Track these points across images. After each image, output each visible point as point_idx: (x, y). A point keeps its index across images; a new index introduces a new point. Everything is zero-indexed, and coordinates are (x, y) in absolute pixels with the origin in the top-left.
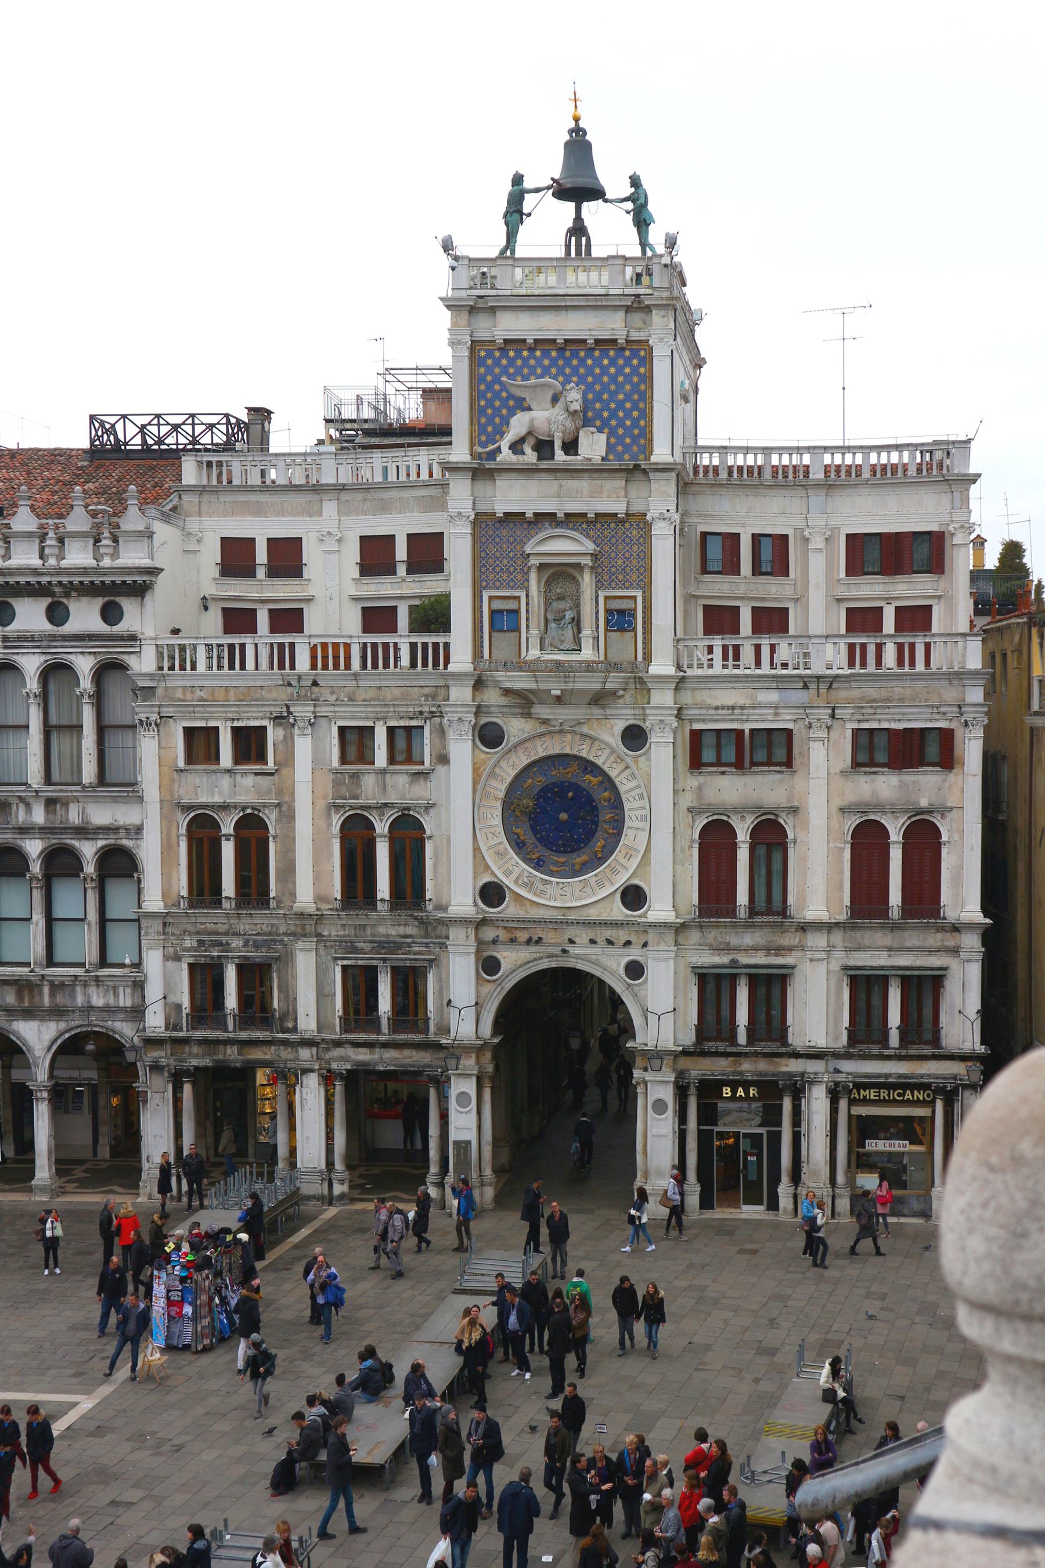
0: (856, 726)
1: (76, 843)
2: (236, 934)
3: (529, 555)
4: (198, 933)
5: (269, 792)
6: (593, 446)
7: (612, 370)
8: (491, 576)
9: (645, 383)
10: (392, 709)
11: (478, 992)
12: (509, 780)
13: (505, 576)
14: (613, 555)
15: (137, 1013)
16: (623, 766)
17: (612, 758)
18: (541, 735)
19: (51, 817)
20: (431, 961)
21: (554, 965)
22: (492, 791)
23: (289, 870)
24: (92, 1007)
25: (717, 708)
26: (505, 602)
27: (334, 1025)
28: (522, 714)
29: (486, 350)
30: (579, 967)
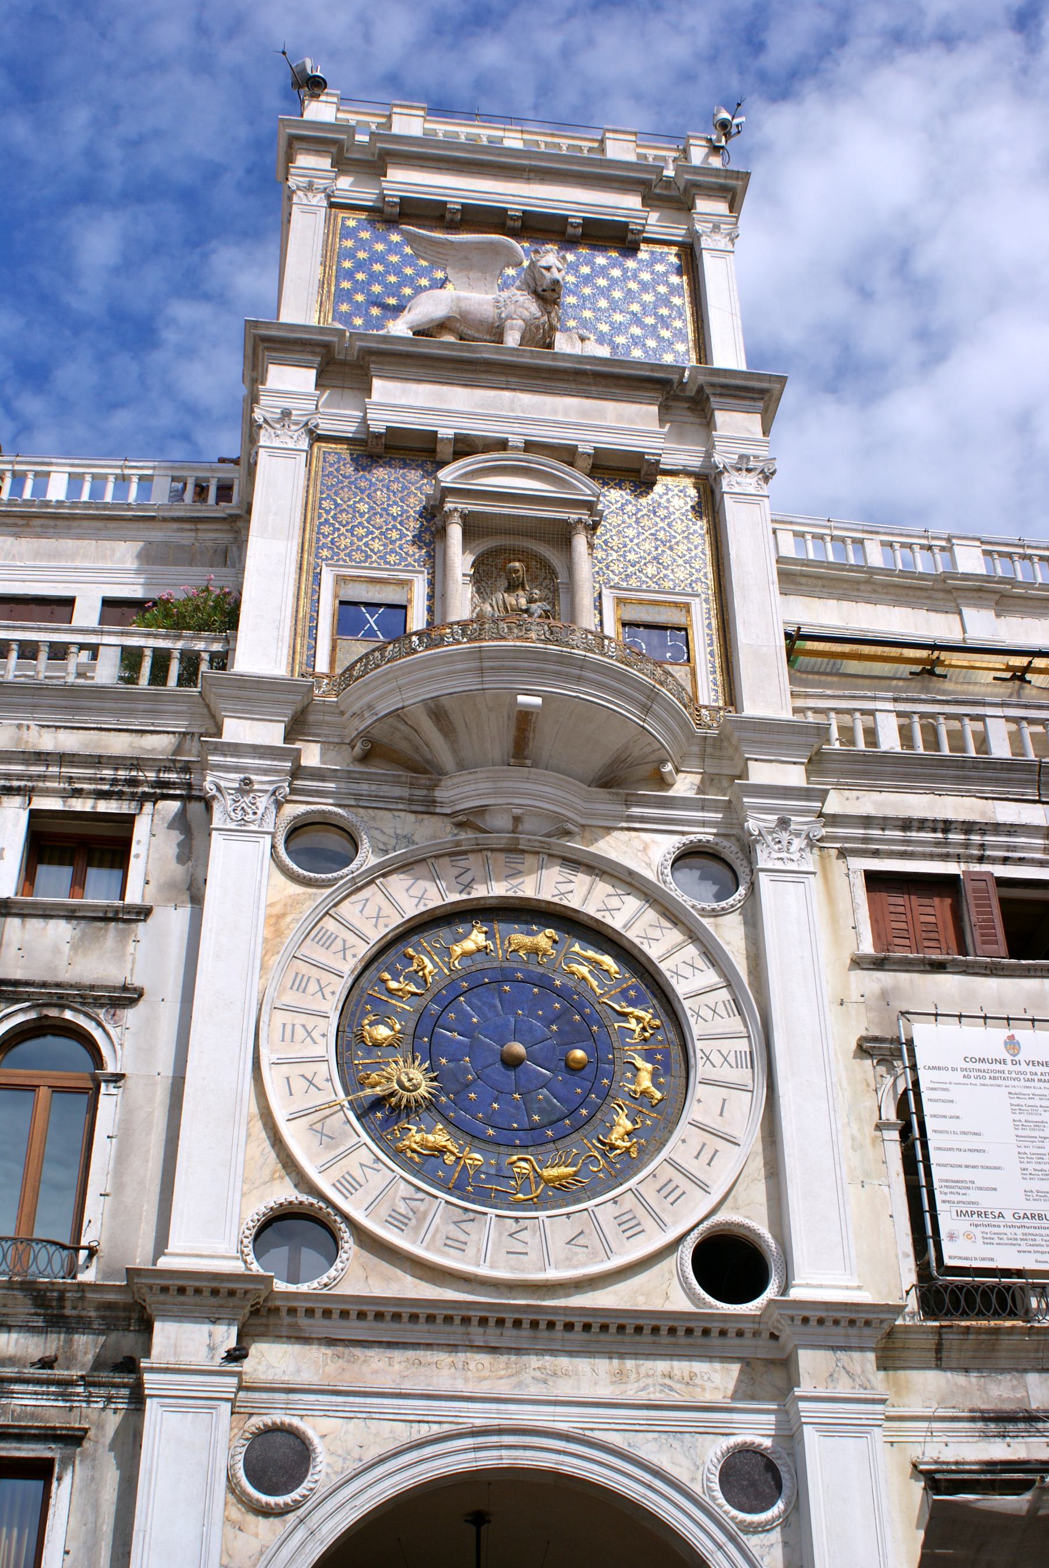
3: (447, 492)
8: (344, 542)
10: (54, 770)
11: (226, 1551)
12: (363, 950)
13: (376, 545)
14: (631, 533)
18: (455, 853)
20: (74, 1439)
21: (488, 1459)
22: (315, 972)
25: (906, 824)
26: (378, 586)
28: (411, 801)
29: (358, 220)
30: (570, 1466)
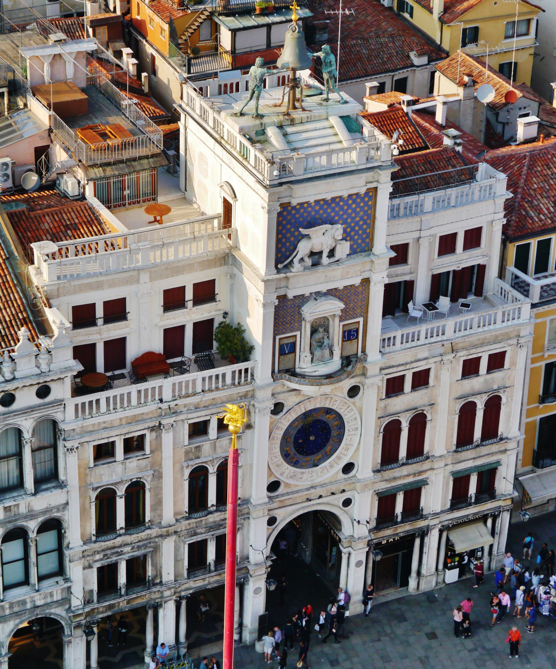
0: (465, 358)
1: (25, 524)
2: (126, 545)
4: (103, 550)
5: (147, 466)
6: (343, 249)
7: (354, 206)
9: (371, 209)
13: (288, 326)
15: (66, 601)
16: (347, 406)
17: (342, 404)
19: (8, 514)
23: (158, 504)
24: (38, 607)
27: (183, 574)
